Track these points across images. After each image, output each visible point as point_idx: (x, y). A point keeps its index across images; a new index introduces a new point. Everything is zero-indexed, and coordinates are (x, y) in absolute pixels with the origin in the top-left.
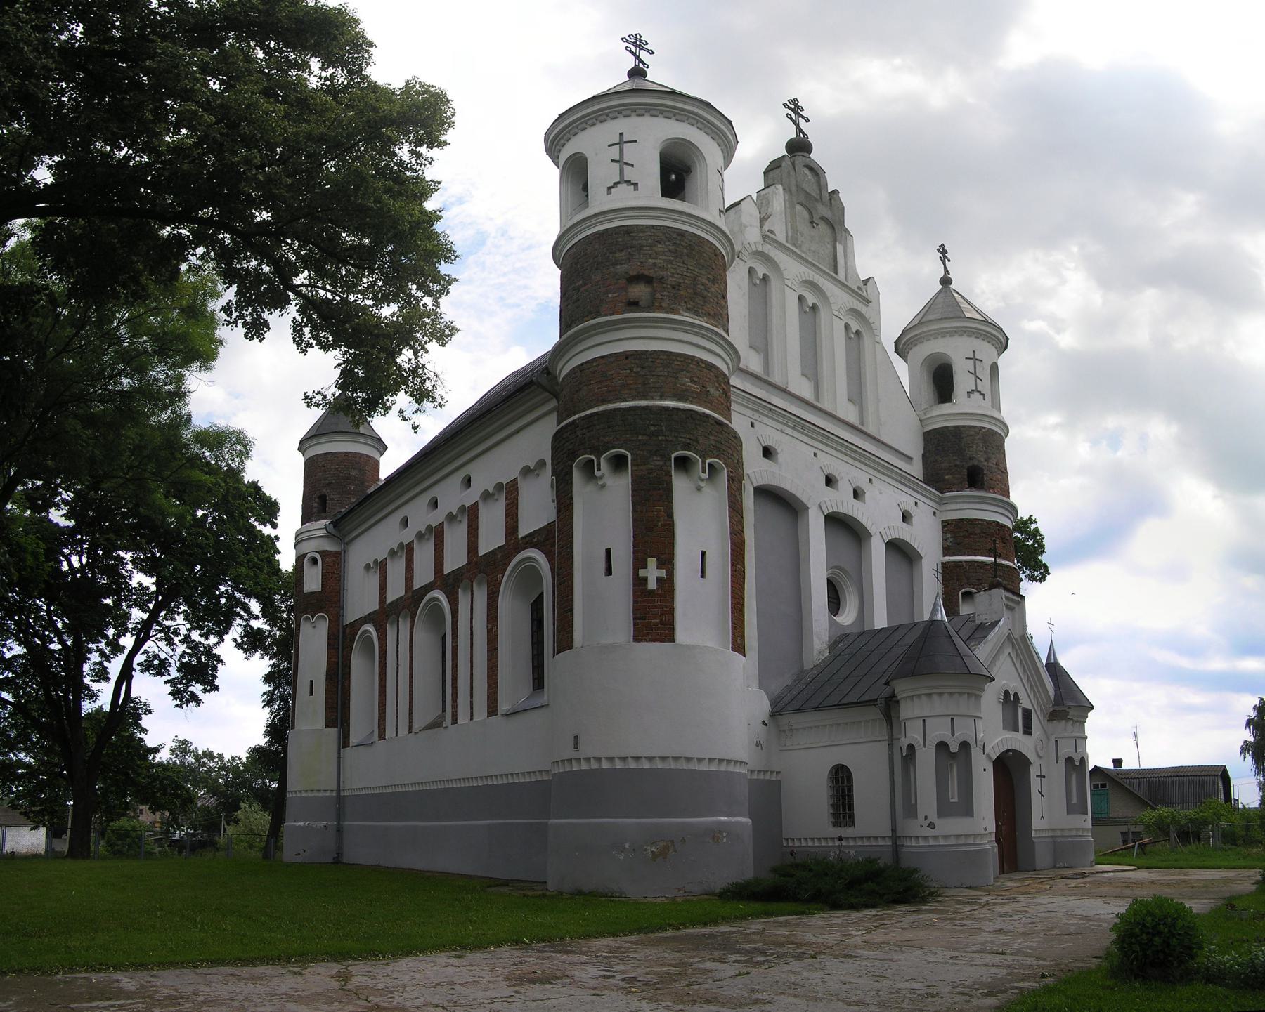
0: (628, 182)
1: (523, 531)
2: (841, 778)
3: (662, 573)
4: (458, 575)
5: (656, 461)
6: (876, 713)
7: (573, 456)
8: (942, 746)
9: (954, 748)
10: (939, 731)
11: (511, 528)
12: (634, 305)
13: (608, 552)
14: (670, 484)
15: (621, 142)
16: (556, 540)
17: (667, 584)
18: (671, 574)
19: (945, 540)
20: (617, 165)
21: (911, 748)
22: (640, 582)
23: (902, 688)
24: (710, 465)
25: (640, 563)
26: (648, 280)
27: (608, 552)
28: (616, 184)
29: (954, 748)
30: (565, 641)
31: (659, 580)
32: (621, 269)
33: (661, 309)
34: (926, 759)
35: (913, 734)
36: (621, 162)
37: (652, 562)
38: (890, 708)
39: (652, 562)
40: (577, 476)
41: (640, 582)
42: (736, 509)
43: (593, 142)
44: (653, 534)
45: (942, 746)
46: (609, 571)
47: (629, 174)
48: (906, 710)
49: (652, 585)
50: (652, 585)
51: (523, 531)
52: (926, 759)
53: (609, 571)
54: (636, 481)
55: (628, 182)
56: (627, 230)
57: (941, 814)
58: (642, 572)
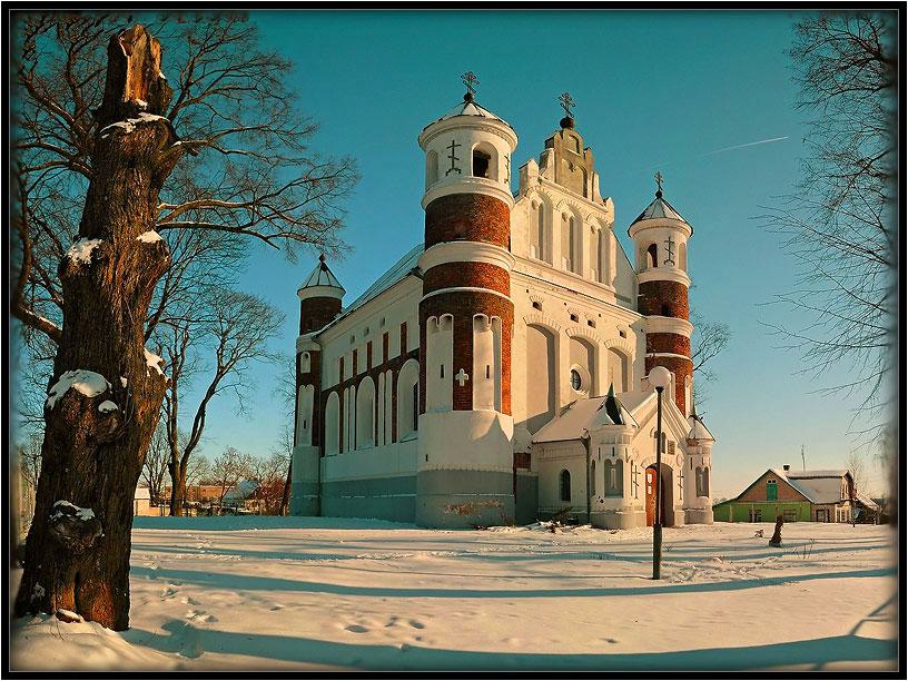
0: (457, 169)
8: (608, 462)
9: (614, 463)
15: (453, 146)
17: (469, 383)
18: (471, 377)
21: (594, 462)
22: (456, 383)
25: (456, 372)
29: (614, 463)
30: (423, 411)
41: (456, 383)
43: (441, 144)
44: (463, 358)
46: (442, 376)
49: (462, 384)
50: (462, 384)
53: (442, 376)
55: (457, 169)
57: (606, 495)
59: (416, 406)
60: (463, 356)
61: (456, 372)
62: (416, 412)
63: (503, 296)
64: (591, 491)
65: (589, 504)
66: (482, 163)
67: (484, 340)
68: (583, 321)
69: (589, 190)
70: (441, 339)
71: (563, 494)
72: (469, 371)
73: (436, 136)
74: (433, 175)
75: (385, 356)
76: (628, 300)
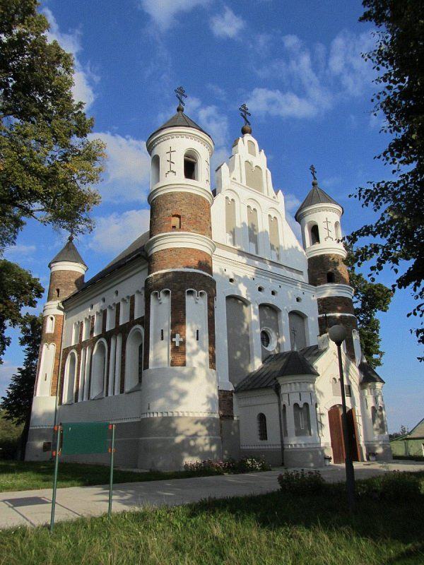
2: (262, 418)
5: (180, 293)
6: (272, 391)
7: (151, 291)
10: (295, 399)
14: (185, 302)
21: (284, 406)
23: (281, 380)
26: (179, 217)
29: (301, 406)
33: (183, 230)
34: (290, 412)
35: (285, 401)
38: (277, 389)
40: (152, 297)
41: (173, 343)
42: (211, 309)
45: (296, 405)
48: (284, 390)
49: (177, 344)
52: (290, 412)
54: (172, 299)
56: (172, 194)
58: (174, 340)
59: (140, 363)
61: (173, 336)
62: (140, 368)
63: (207, 275)
64: (283, 433)
65: (282, 441)
68: (268, 292)
71: (261, 435)
75: (117, 322)
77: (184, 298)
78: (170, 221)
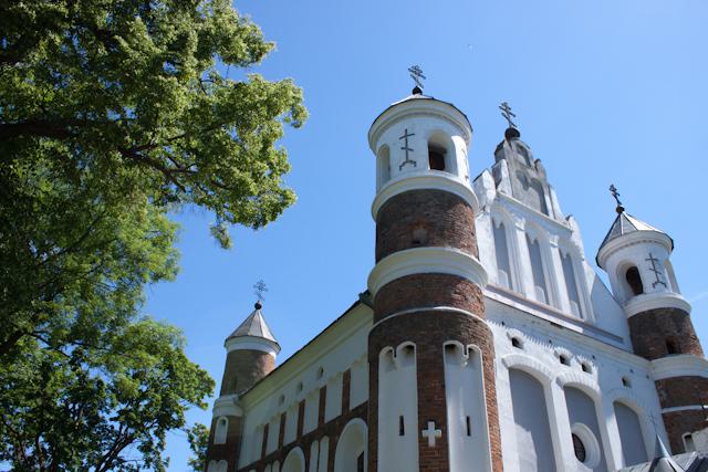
1: (353, 406)
3: (439, 433)
4: (312, 437)
5: (433, 348)
11: (346, 404)
12: (417, 243)
13: (402, 419)
15: (406, 136)
16: (369, 412)
17: (443, 442)
18: (445, 433)
19: (660, 395)
20: (404, 151)
22: (423, 441)
24: (470, 349)
25: (423, 426)
27: (402, 419)
28: (404, 164)
31: (437, 440)
32: (409, 219)
36: (406, 149)
37: (431, 425)
39: (431, 425)
41: (423, 441)
43: (392, 137)
46: (402, 433)
47: (412, 156)
49: (432, 443)
50: (432, 443)
51: (353, 406)
53: (402, 433)
58: (425, 433)
60: (432, 408)
66: (439, 157)
67: (455, 373)
69: (549, 206)
70: (399, 382)
72: (442, 424)
73: (383, 131)
74: (385, 171)
76: (620, 340)
77: (441, 357)
78: (411, 232)
